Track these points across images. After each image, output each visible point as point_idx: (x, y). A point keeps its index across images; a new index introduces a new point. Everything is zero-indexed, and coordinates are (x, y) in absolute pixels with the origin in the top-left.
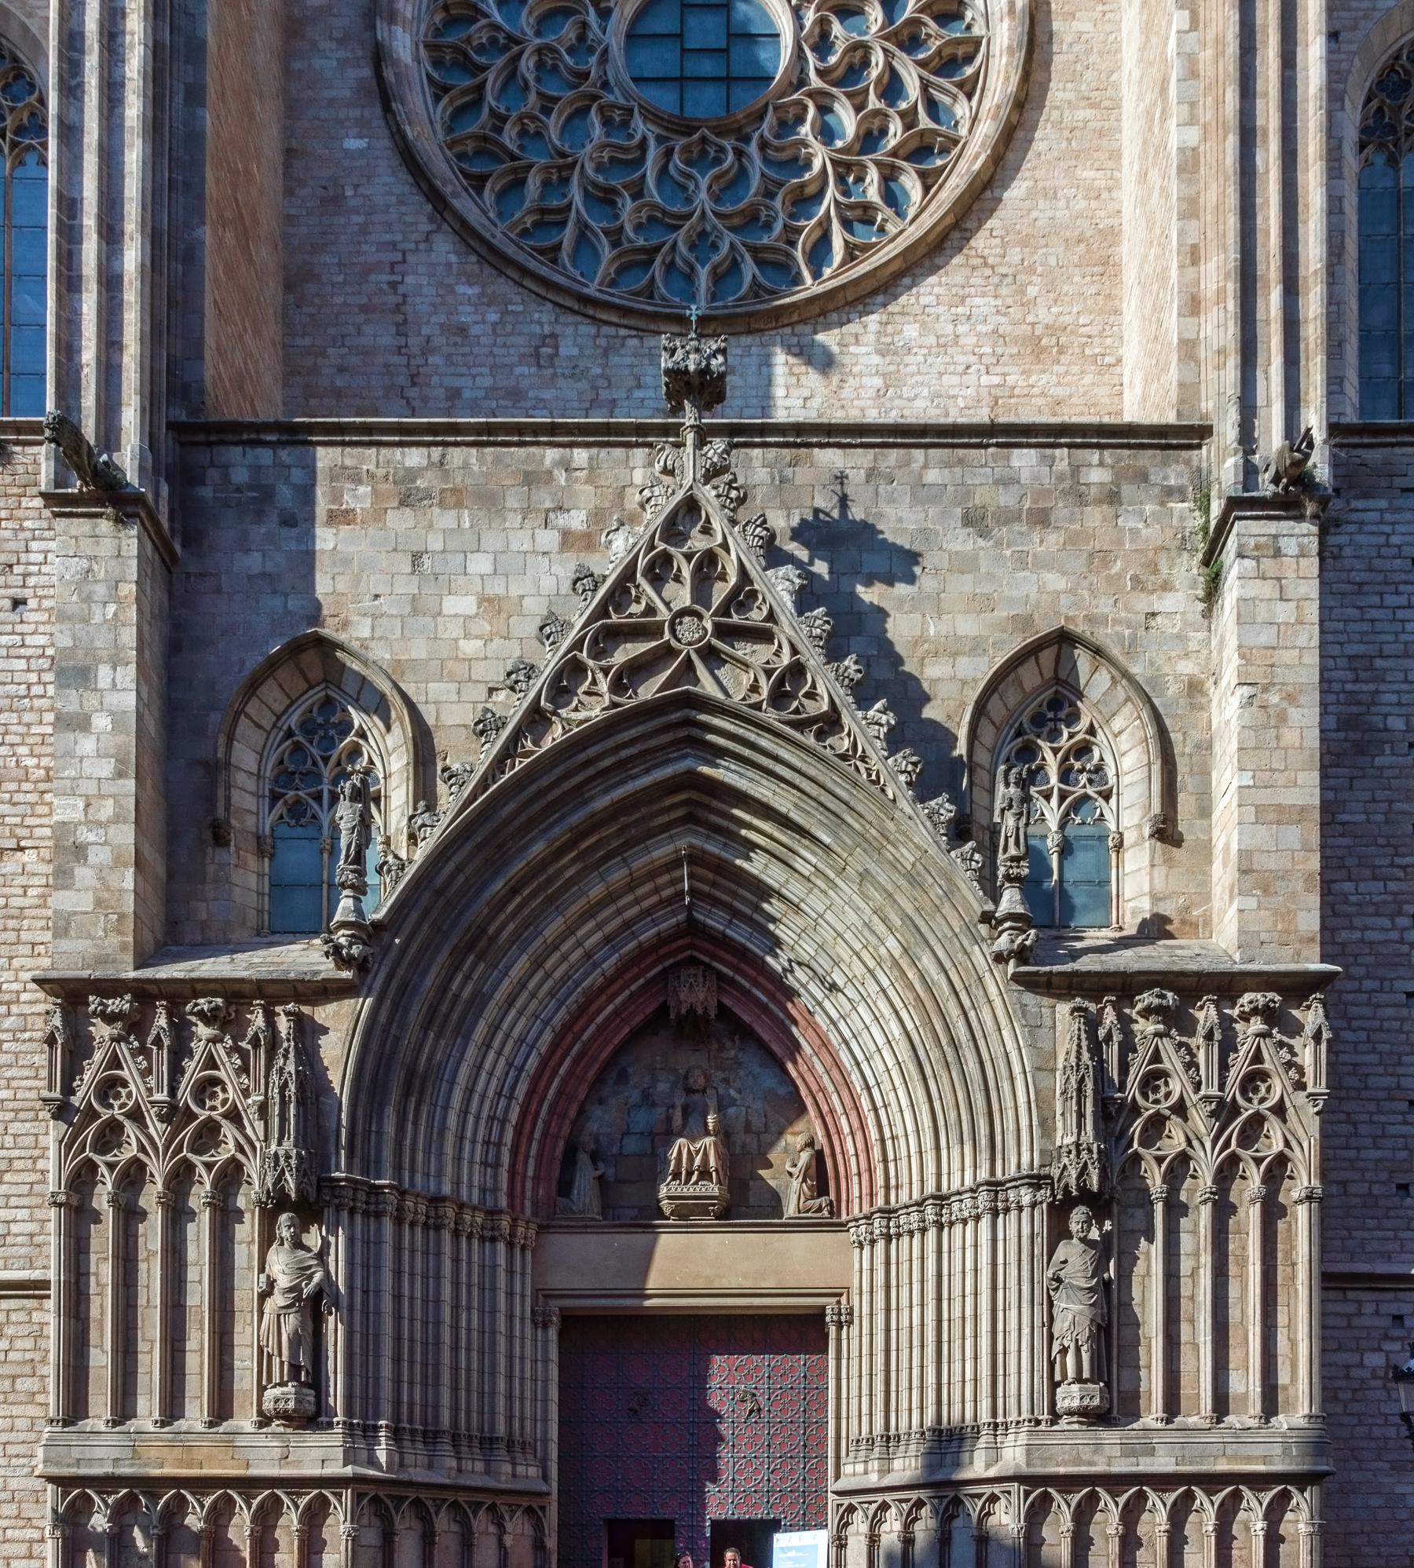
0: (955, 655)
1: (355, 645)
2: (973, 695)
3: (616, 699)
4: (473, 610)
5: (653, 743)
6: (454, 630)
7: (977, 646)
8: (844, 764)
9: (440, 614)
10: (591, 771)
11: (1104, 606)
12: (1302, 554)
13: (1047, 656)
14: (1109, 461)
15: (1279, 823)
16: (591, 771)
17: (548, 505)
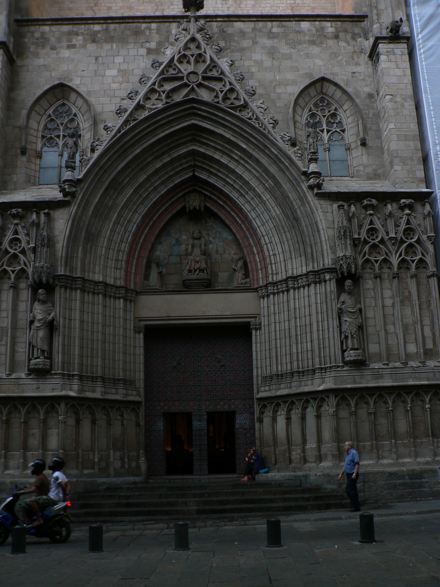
0: (287, 85)
1: (74, 87)
2: (293, 98)
3: (167, 101)
4: (116, 74)
5: (180, 115)
6: (110, 80)
7: (294, 82)
8: (250, 121)
9: (104, 76)
10: (157, 125)
11: (337, 70)
12: (402, 54)
13: (318, 85)
14: (333, 25)
15: (406, 140)
16: (157, 125)
17: (143, 41)
